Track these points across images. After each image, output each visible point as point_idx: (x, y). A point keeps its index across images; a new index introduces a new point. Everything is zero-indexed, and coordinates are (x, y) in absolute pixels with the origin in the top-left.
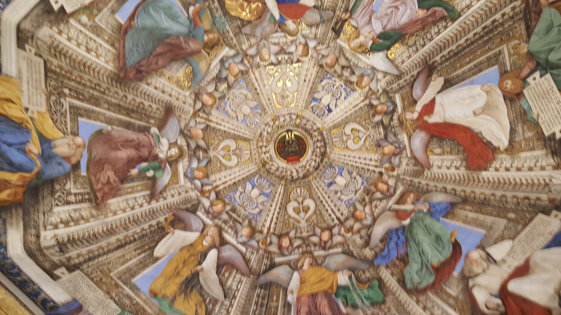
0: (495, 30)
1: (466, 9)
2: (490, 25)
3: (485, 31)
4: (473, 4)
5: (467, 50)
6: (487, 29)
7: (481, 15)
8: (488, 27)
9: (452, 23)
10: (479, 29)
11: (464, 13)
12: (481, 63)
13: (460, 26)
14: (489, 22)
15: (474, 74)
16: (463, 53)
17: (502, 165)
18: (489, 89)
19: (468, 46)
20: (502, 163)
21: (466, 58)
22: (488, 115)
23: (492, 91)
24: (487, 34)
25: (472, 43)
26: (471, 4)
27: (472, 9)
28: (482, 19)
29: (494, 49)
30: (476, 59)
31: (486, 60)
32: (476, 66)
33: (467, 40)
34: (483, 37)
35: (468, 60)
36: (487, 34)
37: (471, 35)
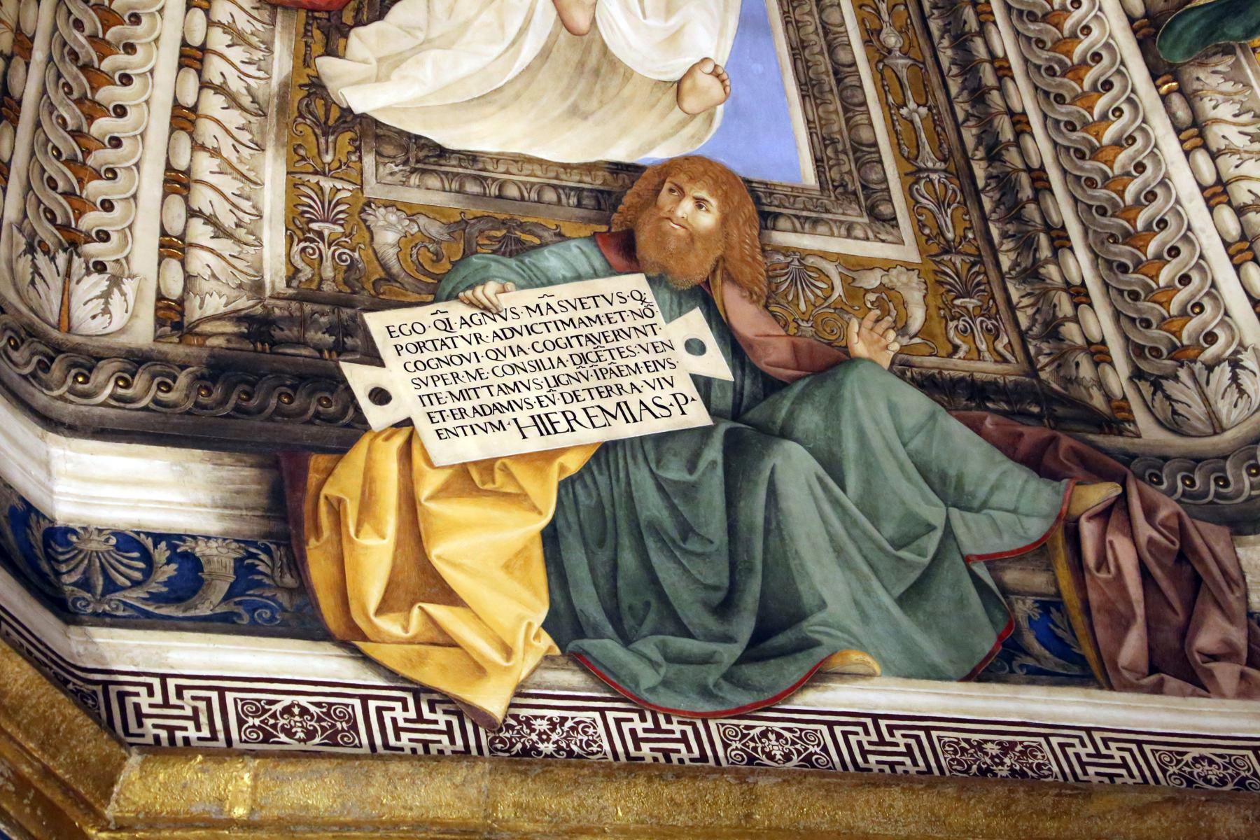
0: (1011, 228)
1: (1183, 114)
2: (1044, 215)
3: (1024, 178)
4: (1201, 158)
5: (946, 55)
6: (1027, 192)
7: (1117, 183)
8: (1036, 200)
9: (1131, 19)
10: (1040, 146)
11: (1164, 98)
12: (853, 106)
13: (1097, 57)
14: (1065, 212)
15: (798, 50)
16: (935, 26)
17: (227, 39)
18: (690, 103)
19: (968, 67)
20: (239, 38)
21: (902, 31)
22: (545, 54)
23: (677, 115)
24: (1005, 183)
25: (978, 95)
26: (1205, 146)
27: (1171, 147)
28: (1091, 183)
29: (910, 192)
30: (883, 90)
31: (865, 135)
32: (843, 72)
33: (1003, 70)
34: (994, 154)
35: (892, 39)
36: (1005, 183)
37: (1023, 96)
